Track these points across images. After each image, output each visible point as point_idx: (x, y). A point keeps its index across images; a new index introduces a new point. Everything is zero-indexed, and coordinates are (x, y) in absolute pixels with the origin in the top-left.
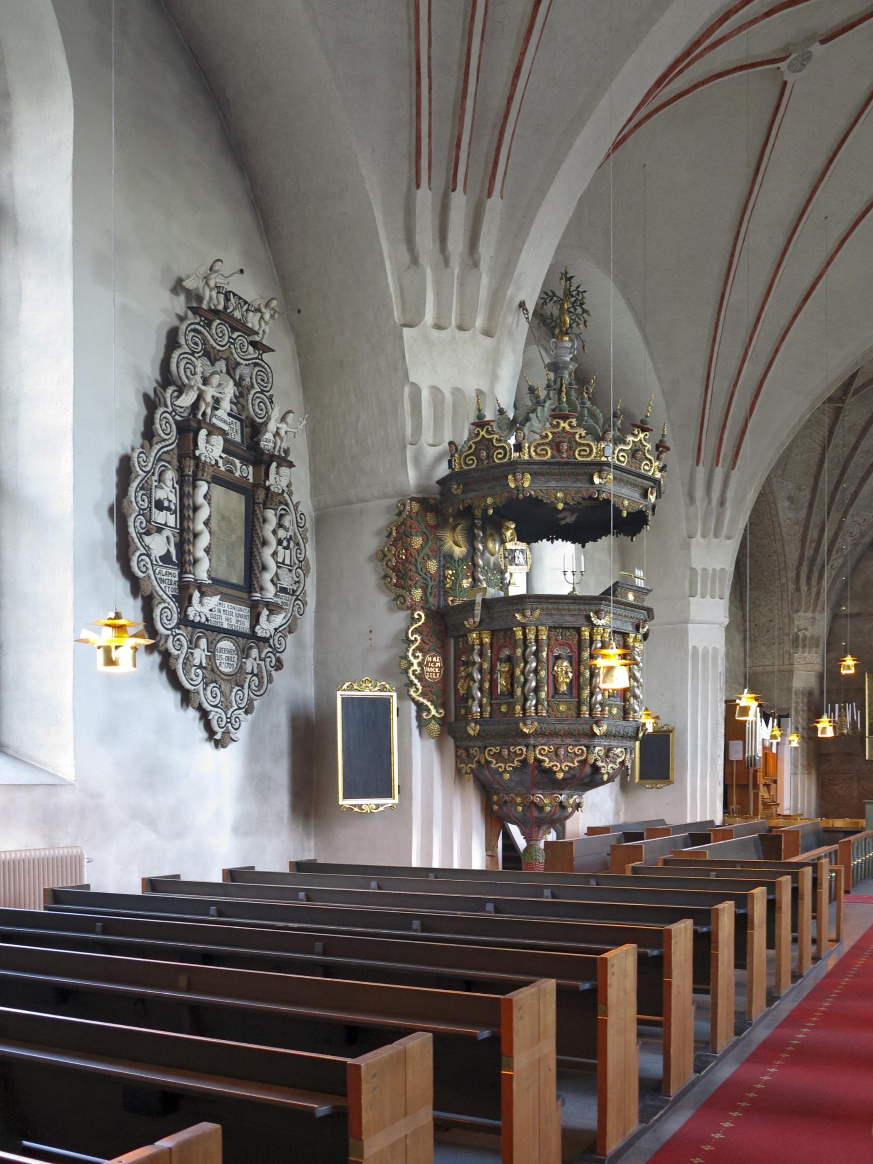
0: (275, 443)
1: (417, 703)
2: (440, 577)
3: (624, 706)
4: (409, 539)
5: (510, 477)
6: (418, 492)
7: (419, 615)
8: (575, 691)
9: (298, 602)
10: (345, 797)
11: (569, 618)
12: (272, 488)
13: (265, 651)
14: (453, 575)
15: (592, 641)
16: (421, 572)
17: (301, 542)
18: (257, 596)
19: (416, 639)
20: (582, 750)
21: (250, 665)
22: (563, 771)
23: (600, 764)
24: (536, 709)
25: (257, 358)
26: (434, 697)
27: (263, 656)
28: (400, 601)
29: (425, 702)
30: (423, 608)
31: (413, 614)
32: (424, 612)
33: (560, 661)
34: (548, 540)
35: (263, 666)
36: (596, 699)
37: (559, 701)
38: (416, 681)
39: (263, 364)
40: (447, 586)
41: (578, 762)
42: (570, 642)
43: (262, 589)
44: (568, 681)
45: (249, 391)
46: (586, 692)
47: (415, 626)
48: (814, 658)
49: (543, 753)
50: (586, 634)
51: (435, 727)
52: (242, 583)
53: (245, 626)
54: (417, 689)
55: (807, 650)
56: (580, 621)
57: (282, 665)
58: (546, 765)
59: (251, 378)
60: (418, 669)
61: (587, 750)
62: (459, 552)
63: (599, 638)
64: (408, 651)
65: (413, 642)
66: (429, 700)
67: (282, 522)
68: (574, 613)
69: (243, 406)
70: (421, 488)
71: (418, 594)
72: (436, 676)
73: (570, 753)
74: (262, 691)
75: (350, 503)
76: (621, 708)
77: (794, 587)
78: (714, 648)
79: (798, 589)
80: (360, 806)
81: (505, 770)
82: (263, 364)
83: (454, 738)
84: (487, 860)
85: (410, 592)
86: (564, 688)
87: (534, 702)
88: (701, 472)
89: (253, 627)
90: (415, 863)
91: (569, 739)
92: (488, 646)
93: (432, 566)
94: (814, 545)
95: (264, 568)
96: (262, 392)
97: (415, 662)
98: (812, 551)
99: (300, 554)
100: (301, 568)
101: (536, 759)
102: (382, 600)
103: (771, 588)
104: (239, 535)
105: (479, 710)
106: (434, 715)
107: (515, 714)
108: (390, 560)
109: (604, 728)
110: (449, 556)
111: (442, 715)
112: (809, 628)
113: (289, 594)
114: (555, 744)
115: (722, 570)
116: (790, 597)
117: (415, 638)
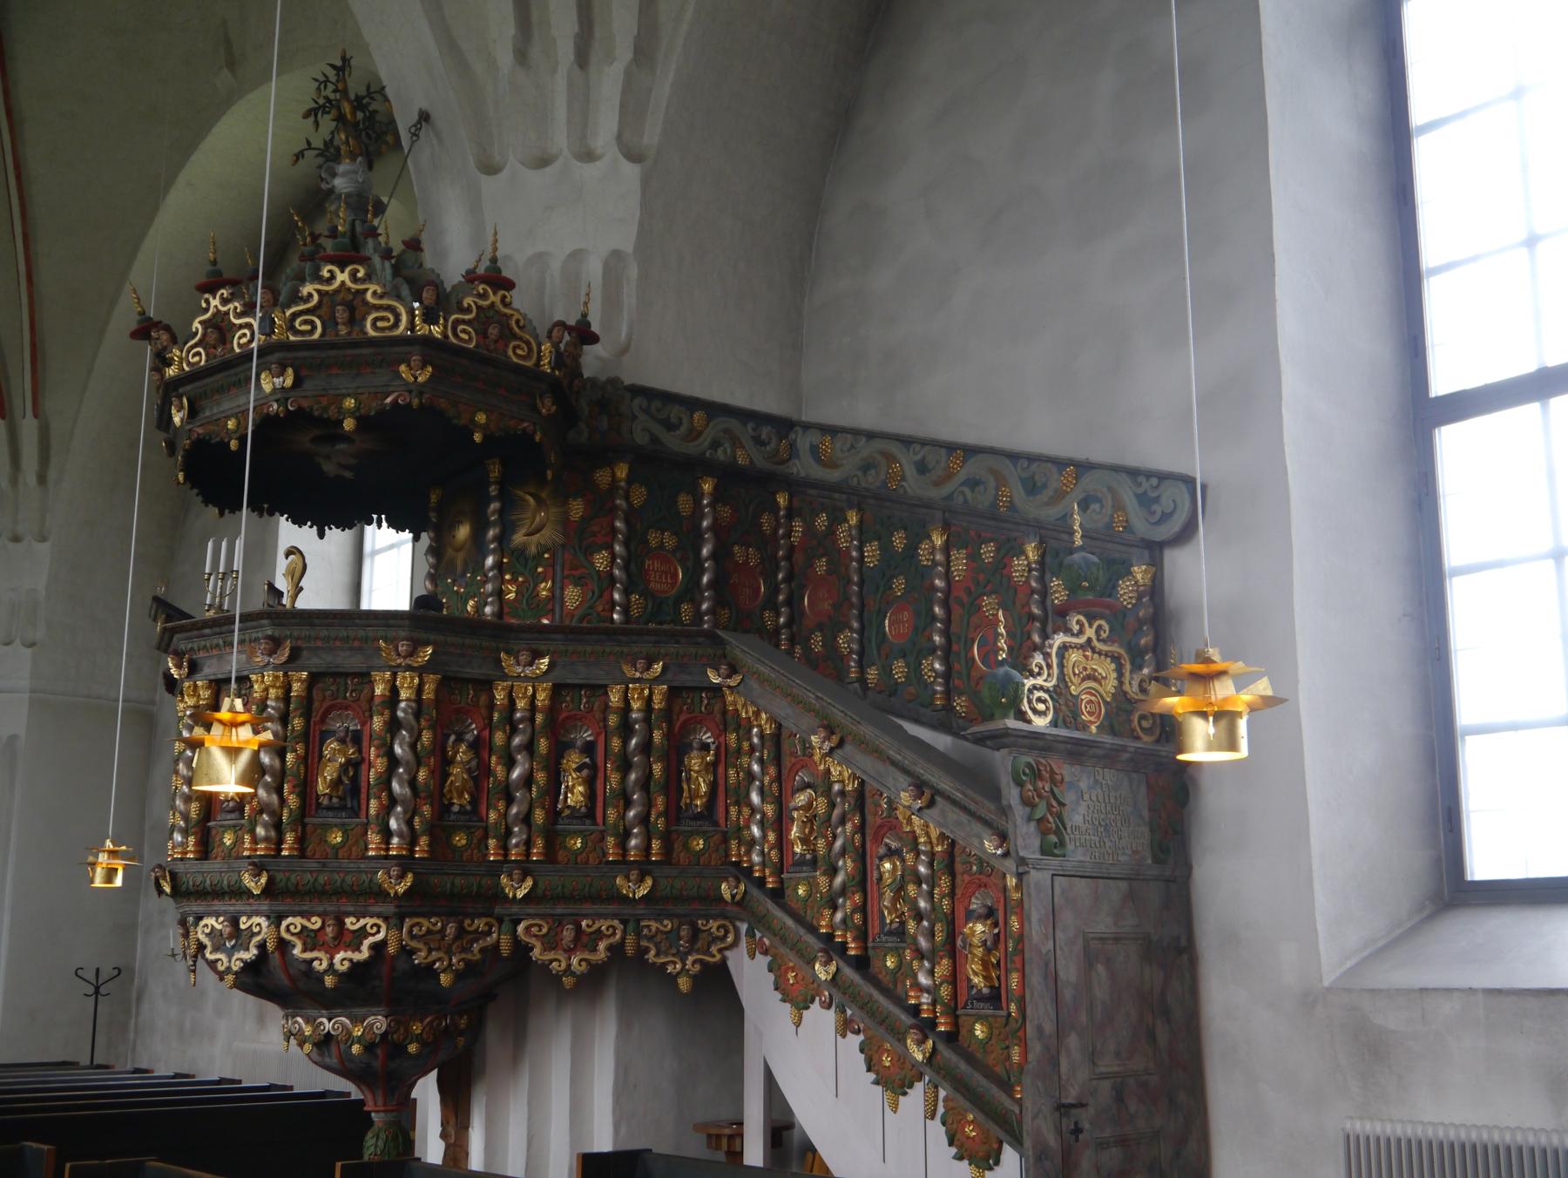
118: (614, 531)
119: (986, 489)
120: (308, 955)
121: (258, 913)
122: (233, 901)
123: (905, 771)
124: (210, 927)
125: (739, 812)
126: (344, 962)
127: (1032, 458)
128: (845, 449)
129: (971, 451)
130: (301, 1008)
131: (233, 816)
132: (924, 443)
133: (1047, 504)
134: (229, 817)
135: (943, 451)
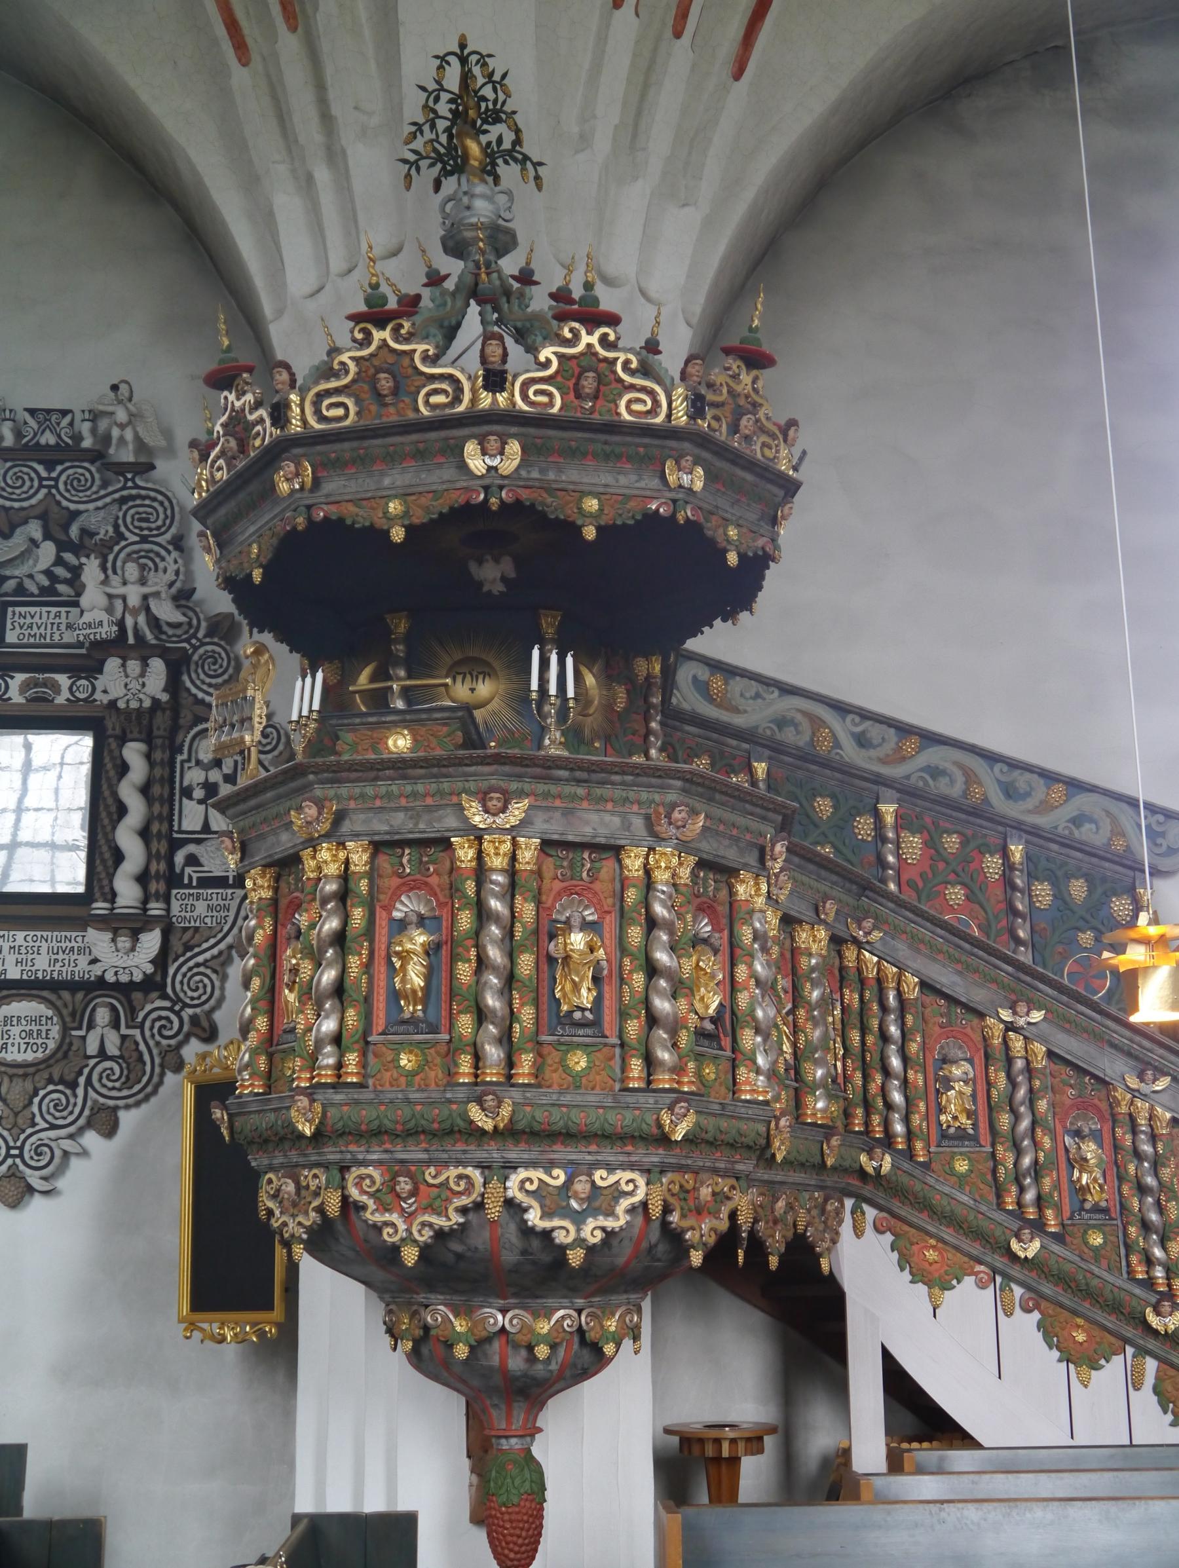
0: (121, 624)
12: (121, 704)
35: (139, 1038)
39: (143, 492)
82: (143, 492)
96: (144, 539)
118: (649, 732)
119: (952, 782)
120: (547, 1224)
121: (632, 1167)
122: (593, 1148)
123: (1129, 1054)
124: (536, 1183)
125: (866, 1078)
126: (595, 1233)
127: (1014, 765)
128: (748, 695)
129: (931, 739)
130: (537, 1297)
131: (589, 1031)
132: (865, 715)
133: (1029, 812)
134: (581, 1032)
135: (892, 731)
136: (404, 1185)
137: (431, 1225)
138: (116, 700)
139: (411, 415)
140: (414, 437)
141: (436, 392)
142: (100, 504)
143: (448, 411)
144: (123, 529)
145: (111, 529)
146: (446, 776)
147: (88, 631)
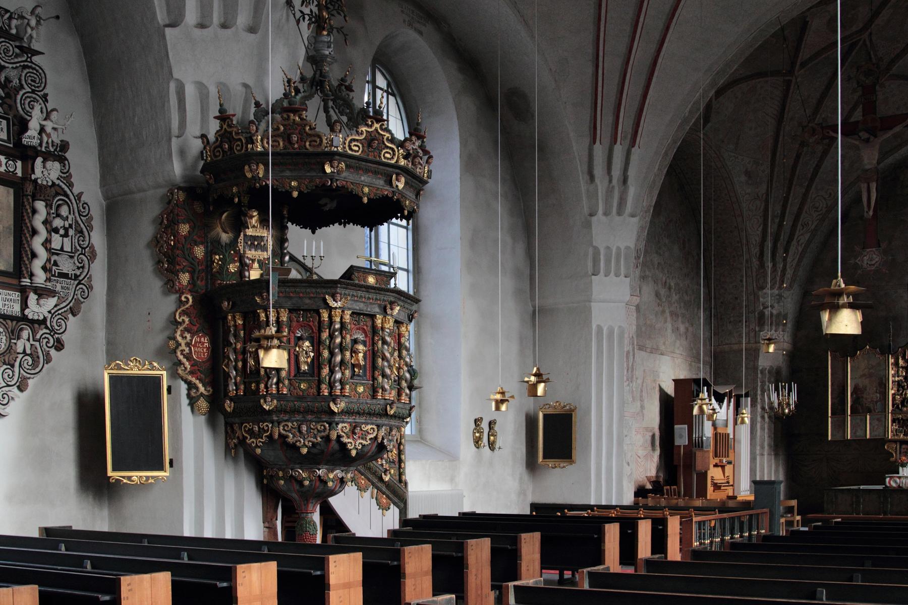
0: (41, 140)
1: (186, 381)
2: (207, 261)
3: (373, 385)
4: (176, 226)
5: (247, 167)
6: (185, 182)
7: (186, 298)
8: (316, 371)
9: (81, 286)
10: (114, 469)
11: (307, 301)
12: (39, 181)
13: (41, 332)
14: (220, 259)
15: (331, 321)
16: (187, 257)
17: (84, 229)
18: (26, 281)
19: (184, 321)
20: (324, 426)
21: (20, 346)
22: (307, 446)
23: (345, 440)
24: (278, 388)
25: (26, 61)
26: (202, 375)
27: (38, 337)
28: (170, 286)
29: (194, 380)
30: (190, 291)
31: (180, 297)
32: (191, 295)
33: (300, 343)
34: (340, 224)
36: (335, 378)
37: (301, 380)
38: (184, 360)
39: (34, 66)
40: (214, 270)
41: (321, 438)
42: (311, 324)
43: (31, 275)
44: (309, 360)
45: (18, 92)
46: (325, 371)
47: (183, 308)
48: (781, 337)
49: (286, 429)
50: (325, 316)
51: (203, 404)
52: (11, 270)
53: (16, 309)
54: (186, 368)
55: (774, 328)
56: (321, 303)
57: (63, 346)
58: (289, 440)
59: (20, 80)
60: (187, 350)
61: (329, 426)
62: (225, 237)
63: (338, 319)
64: (176, 332)
65: (180, 324)
66: (197, 379)
67: (59, 212)
68: (312, 295)
69: (10, 107)
70: (187, 178)
71: (185, 278)
72: (204, 355)
73: (313, 429)
74: (37, 370)
75: (132, 192)
76: (369, 386)
77: (758, 263)
78: (620, 327)
79: (762, 265)
80: (129, 478)
81: (257, 446)
82: (34, 66)
83: (223, 414)
84: (264, 532)
85: (178, 276)
86: (304, 367)
87: (275, 380)
88: (599, 151)
89: (23, 310)
90: (188, 532)
91: (310, 416)
92: (241, 327)
93: (199, 251)
94: (777, 220)
95: (34, 255)
96: (33, 92)
97: (183, 342)
98: (775, 226)
99: (83, 241)
100: (84, 255)
101: (280, 434)
102: (157, 284)
103: (735, 264)
104: (7, 225)
105: (235, 388)
106: (202, 393)
107: (260, 392)
108: (162, 246)
109: (342, 405)
110: (218, 241)
111: (210, 393)
112: (776, 305)
113: (71, 279)
114: (298, 420)
115: (627, 248)
116: (754, 274)
117: (183, 320)
136: (358, 430)
137: (361, 444)
138: (38, 178)
139: (378, 159)
140: (375, 166)
141: (387, 152)
142: (14, 66)
143: (389, 161)
144: (23, 82)
145: (18, 81)
146: (379, 294)
147: (28, 140)
